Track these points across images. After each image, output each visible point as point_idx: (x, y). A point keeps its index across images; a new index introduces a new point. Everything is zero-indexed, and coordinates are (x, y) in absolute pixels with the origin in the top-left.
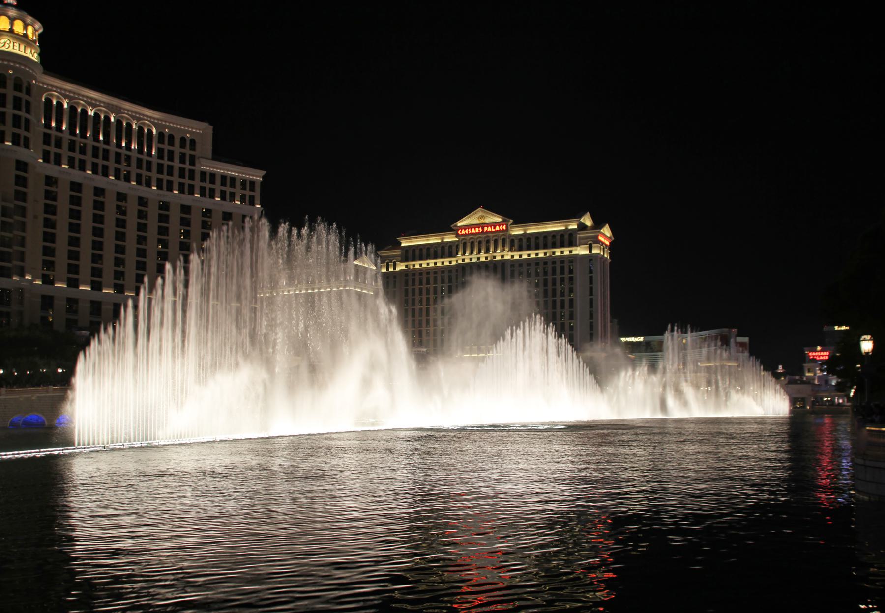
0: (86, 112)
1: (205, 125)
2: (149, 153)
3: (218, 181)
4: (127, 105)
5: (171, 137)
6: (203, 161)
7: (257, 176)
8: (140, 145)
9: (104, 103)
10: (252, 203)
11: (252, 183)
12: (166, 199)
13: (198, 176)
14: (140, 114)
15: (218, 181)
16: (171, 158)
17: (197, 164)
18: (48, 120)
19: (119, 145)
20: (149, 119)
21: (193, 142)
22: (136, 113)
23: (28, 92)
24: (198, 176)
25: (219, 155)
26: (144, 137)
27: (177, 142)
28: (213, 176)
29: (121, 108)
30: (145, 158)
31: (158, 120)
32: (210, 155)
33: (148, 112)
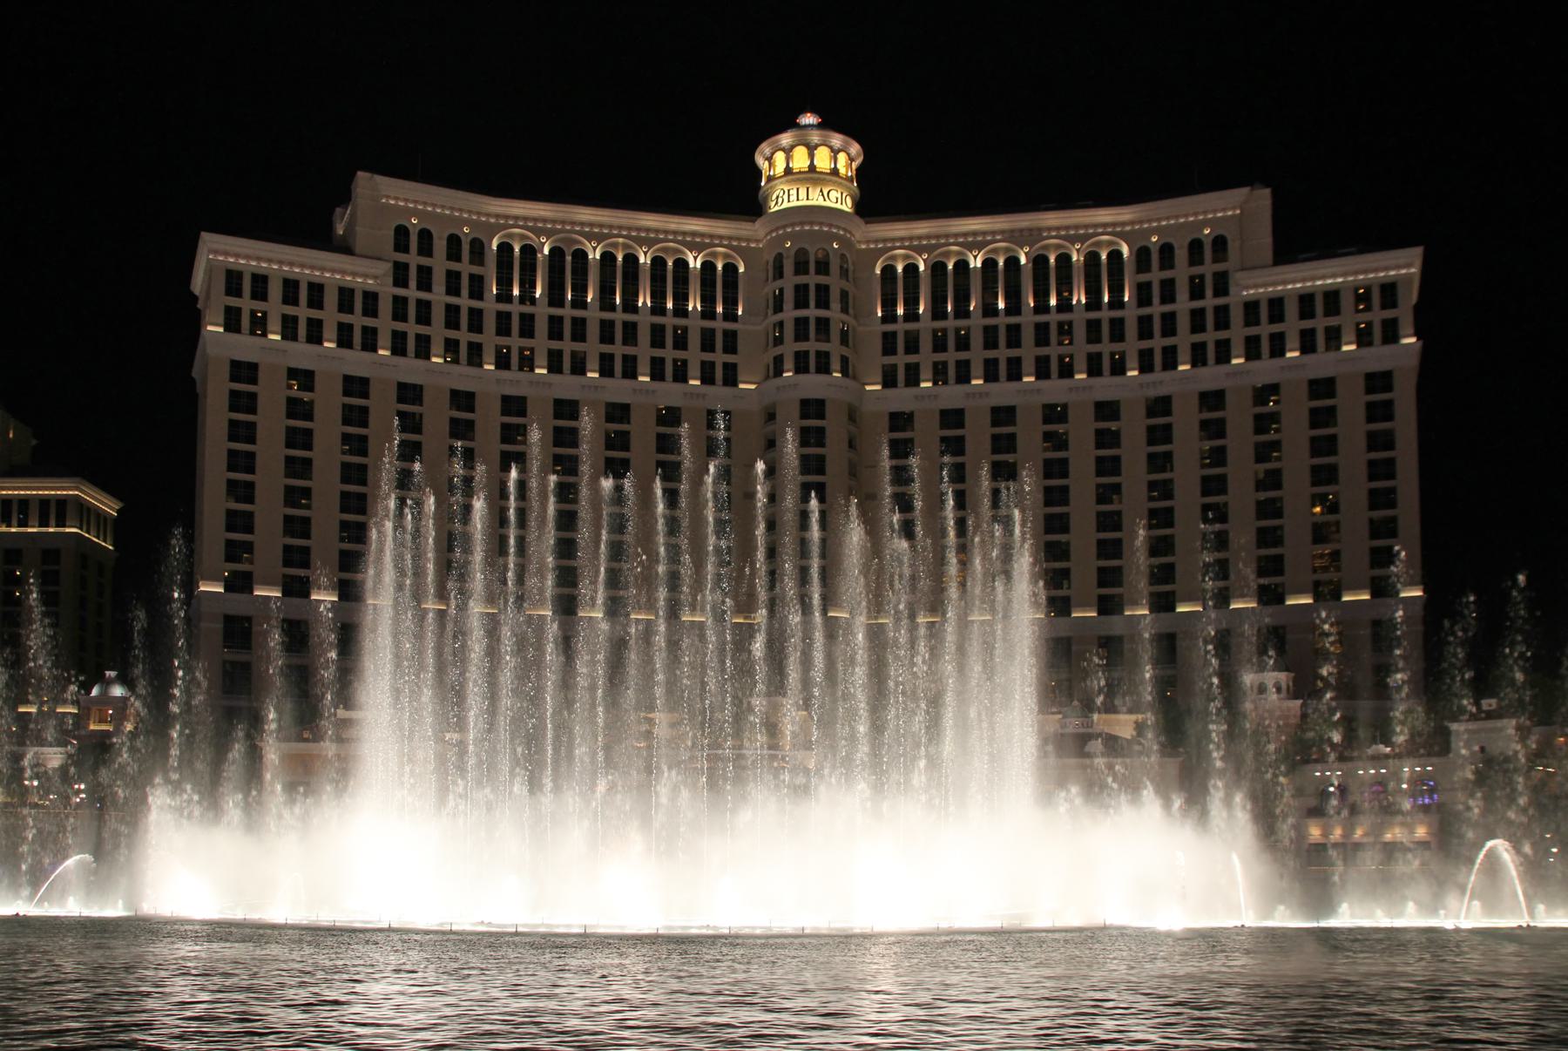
0: (966, 263)
2: (1116, 303)
3: (1291, 310)
4: (1051, 219)
5: (1167, 250)
7: (1403, 266)
8: (1093, 292)
9: (1002, 232)
10: (1391, 334)
11: (1389, 292)
12: (1162, 391)
13: (1237, 316)
14: (1086, 227)
15: (1291, 310)
16: (1168, 293)
17: (1232, 290)
18: (889, 304)
19: (1041, 307)
21: (1220, 243)
22: (1077, 227)
23: (823, 267)
24: (1237, 316)
25: (1287, 250)
27: (1181, 255)
28: (1276, 304)
29: (1040, 230)
30: (1105, 315)
31: (1132, 223)
32: (1268, 255)
33: (1104, 215)
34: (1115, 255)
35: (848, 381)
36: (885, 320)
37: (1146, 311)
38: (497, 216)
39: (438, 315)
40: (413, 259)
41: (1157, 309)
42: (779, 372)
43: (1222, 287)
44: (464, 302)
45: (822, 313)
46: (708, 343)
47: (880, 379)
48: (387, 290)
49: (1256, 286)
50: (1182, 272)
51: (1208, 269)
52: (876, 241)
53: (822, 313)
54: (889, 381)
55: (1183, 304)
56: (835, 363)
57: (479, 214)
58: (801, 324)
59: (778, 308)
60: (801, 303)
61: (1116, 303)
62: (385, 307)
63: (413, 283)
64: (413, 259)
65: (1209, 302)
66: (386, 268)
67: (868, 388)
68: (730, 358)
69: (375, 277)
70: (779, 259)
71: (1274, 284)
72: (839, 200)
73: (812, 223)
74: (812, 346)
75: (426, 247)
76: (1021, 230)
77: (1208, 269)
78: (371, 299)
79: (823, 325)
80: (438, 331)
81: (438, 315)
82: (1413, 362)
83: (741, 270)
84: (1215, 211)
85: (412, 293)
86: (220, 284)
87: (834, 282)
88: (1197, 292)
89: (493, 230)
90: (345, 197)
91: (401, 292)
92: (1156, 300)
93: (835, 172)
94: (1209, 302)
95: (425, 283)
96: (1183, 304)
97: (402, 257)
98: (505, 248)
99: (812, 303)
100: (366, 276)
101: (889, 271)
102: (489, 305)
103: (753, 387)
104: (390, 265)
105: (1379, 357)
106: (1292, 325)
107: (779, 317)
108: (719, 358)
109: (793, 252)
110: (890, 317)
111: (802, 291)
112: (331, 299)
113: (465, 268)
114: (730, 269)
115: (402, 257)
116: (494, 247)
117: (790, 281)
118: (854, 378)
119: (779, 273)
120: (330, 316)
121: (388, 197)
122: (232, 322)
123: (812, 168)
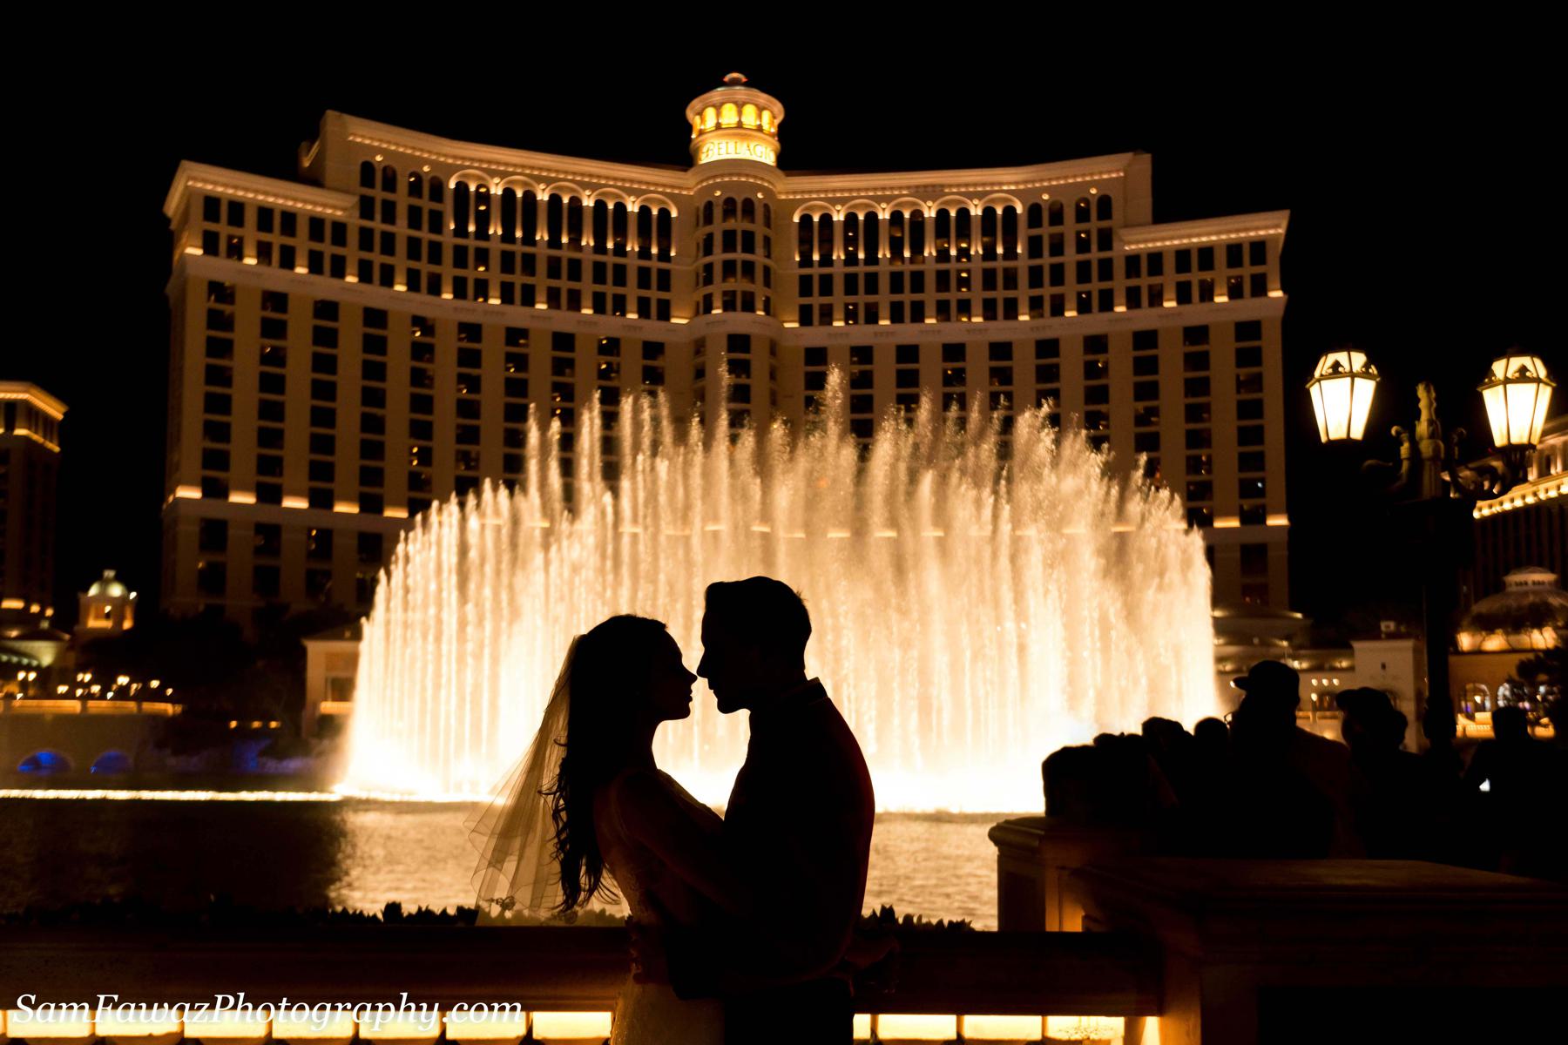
1: (1126, 157)
3: (1169, 264)
6: (1124, 234)
7: (1271, 227)
9: (908, 188)
10: (1260, 288)
11: (1259, 247)
13: (1119, 268)
15: (1169, 264)
16: (1057, 248)
17: (1115, 245)
20: (1004, 186)
24: (1119, 268)
25: (1167, 211)
26: (999, 225)
27: (1069, 214)
28: (1156, 259)
29: (943, 186)
31: (1025, 182)
32: (1149, 218)
34: (1010, 210)
35: (770, 319)
36: (802, 264)
37: (1037, 262)
38: (455, 157)
39: (401, 247)
40: (378, 194)
41: (1046, 260)
42: (708, 308)
43: (1106, 240)
44: (425, 235)
45: (748, 257)
46: (644, 281)
47: (797, 317)
48: (355, 222)
49: (1138, 242)
50: (1070, 228)
51: (1094, 224)
52: (795, 193)
53: (748, 257)
54: (805, 318)
55: (1070, 257)
56: (759, 303)
57: (438, 154)
58: (729, 268)
59: (708, 250)
60: (729, 245)
61: (1010, 253)
62: (353, 238)
63: (378, 216)
64: (378, 194)
65: (1095, 255)
66: (352, 201)
67: (787, 325)
68: (664, 295)
69: (343, 209)
70: (709, 206)
71: (1154, 240)
72: (766, 153)
73: (739, 175)
74: (738, 284)
75: (390, 182)
76: (925, 186)
77: (1094, 224)
78: (339, 229)
79: (749, 268)
80: (400, 262)
81: (401, 247)
82: (1280, 312)
83: (674, 214)
84: (1101, 173)
85: (377, 225)
86: (198, 210)
87: (759, 229)
88: (1083, 246)
89: (452, 170)
90: (313, 132)
91: (367, 223)
92: (1046, 252)
93: (760, 129)
94: (1095, 255)
95: (389, 217)
96: (1070, 257)
97: (368, 192)
98: (462, 187)
99: (739, 248)
100: (334, 207)
101: (806, 219)
102: (448, 238)
103: (684, 321)
104: (355, 199)
105: (1249, 309)
106: (1170, 278)
107: (708, 259)
108: (654, 294)
109: (721, 202)
110: (806, 261)
111: (729, 237)
112: (303, 228)
113: (426, 204)
114: (664, 213)
115: (368, 192)
116: (452, 185)
117: (718, 227)
118: (774, 316)
119: (709, 219)
120: (302, 243)
121: (355, 135)
122: (210, 244)
123: (740, 125)
